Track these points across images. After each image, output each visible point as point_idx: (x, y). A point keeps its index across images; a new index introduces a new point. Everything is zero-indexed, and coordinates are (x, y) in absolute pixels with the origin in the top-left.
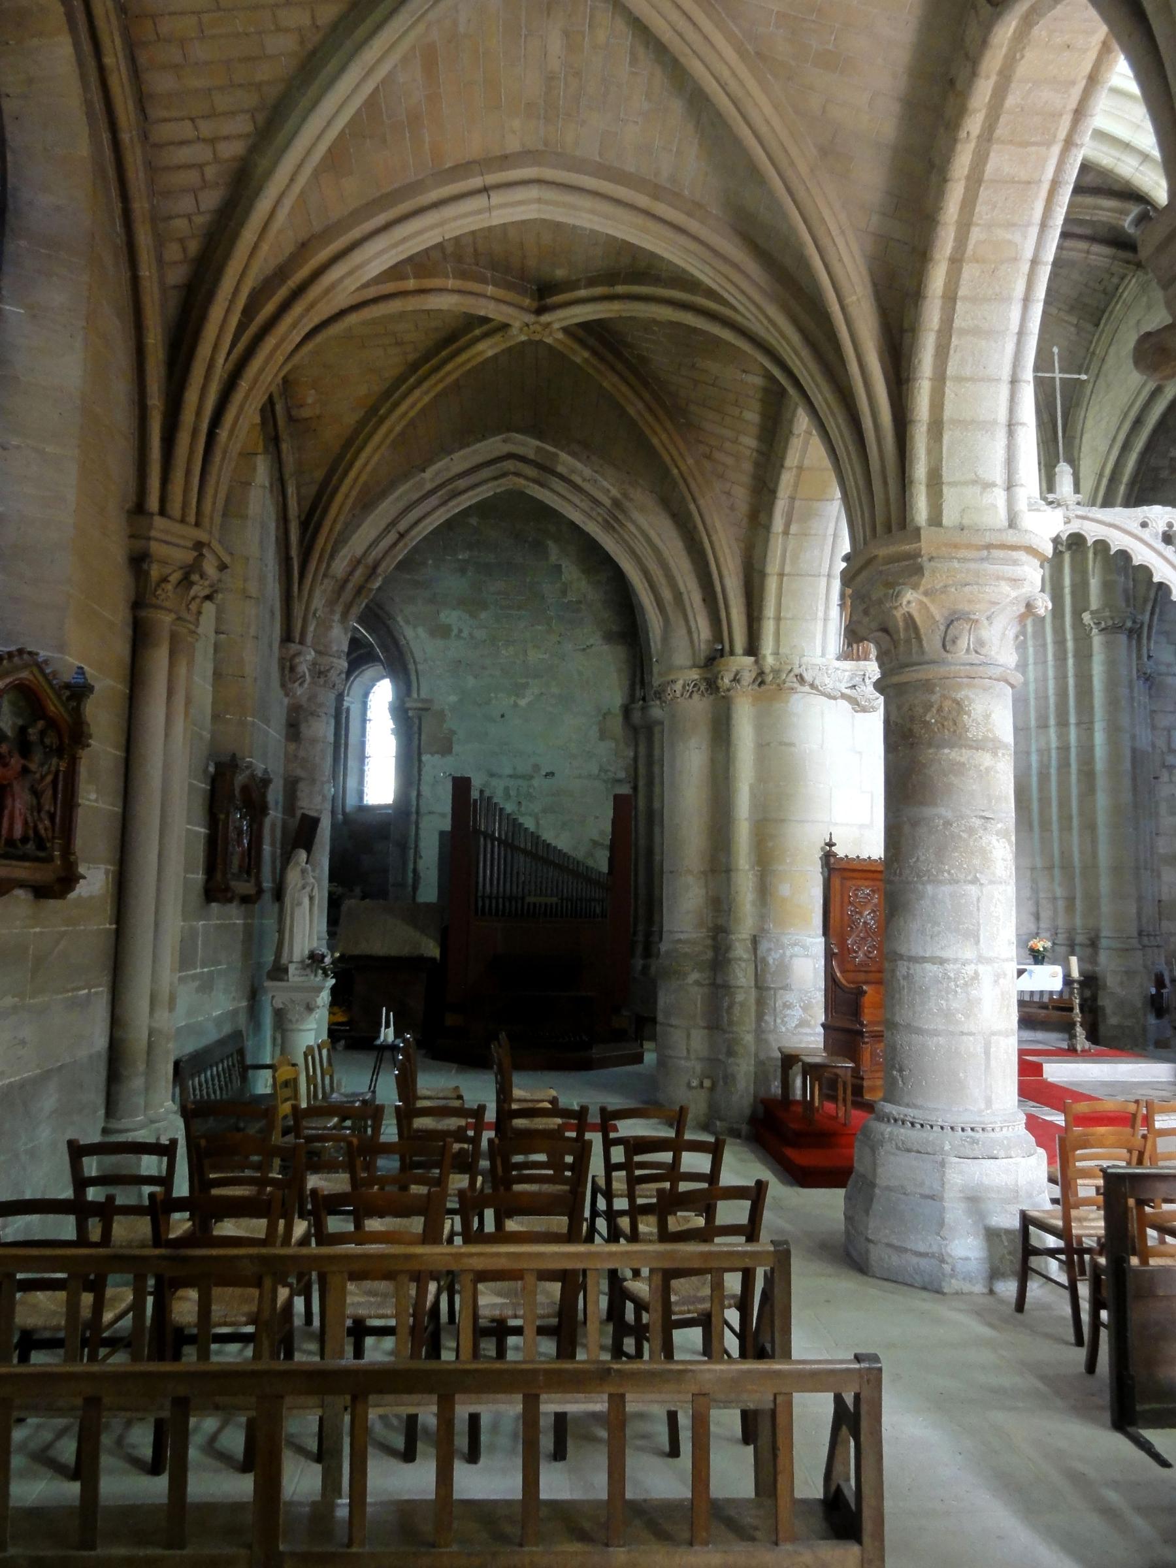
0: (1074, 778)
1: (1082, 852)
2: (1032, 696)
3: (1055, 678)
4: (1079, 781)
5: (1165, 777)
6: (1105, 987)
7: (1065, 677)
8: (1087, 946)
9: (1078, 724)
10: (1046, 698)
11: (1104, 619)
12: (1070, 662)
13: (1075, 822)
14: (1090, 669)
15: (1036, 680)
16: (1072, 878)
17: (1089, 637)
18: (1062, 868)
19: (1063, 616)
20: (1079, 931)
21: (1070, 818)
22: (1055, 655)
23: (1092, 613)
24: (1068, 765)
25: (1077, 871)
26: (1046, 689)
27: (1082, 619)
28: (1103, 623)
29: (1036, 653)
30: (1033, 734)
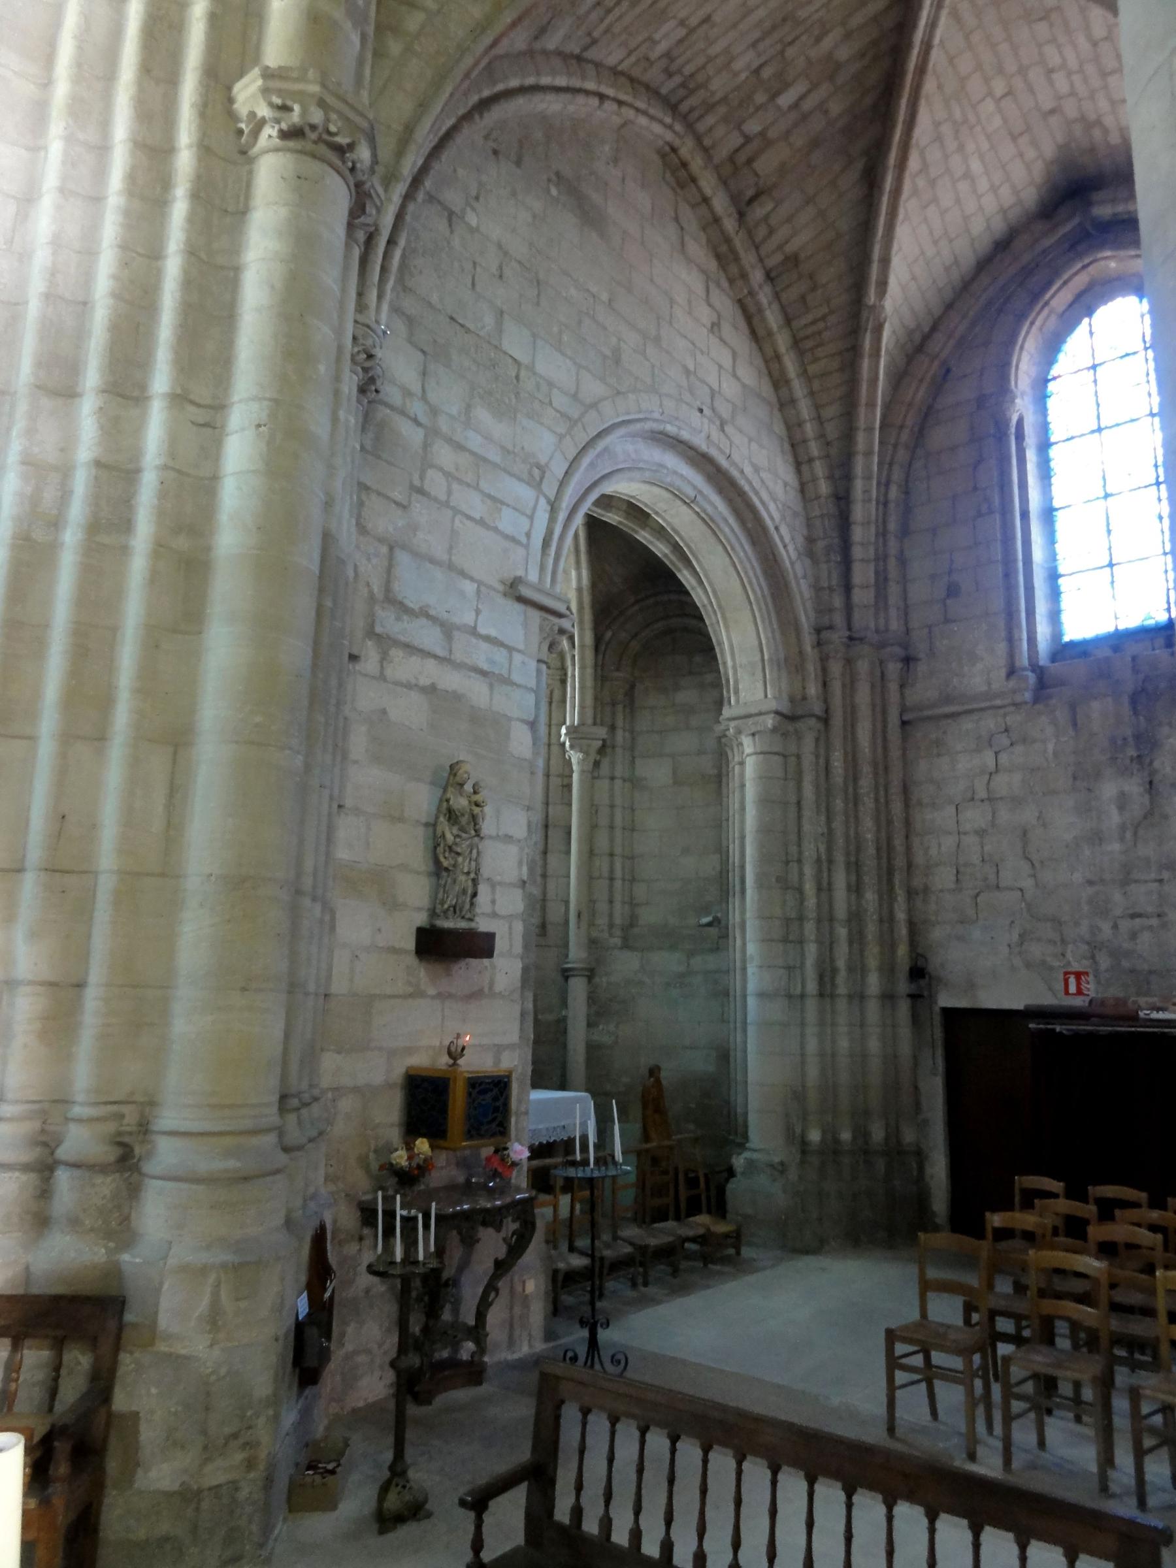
0: (138, 565)
1: (130, 818)
2: (37, 286)
3: (124, 247)
4: (153, 578)
5: (370, 662)
6: (151, 1333)
7: (155, 254)
8: (101, 1169)
9: (179, 399)
10: (84, 305)
11: (300, 96)
12: (179, 209)
13: (122, 716)
14: (236, 248)
15: (56, 243)
16: (83, 910)
17: (244, 156)
18: (51, 869)
19: (172, 80)
20: (77, 1111)
21: (106, 703)
22: (131, 178)
23: (268, 74)
24: (126, 525)
25: (106, 885)
26: (87, 278)
27: (231, 100)
28: (297, 108)
29: (69, 162)
30: (22, 407)
